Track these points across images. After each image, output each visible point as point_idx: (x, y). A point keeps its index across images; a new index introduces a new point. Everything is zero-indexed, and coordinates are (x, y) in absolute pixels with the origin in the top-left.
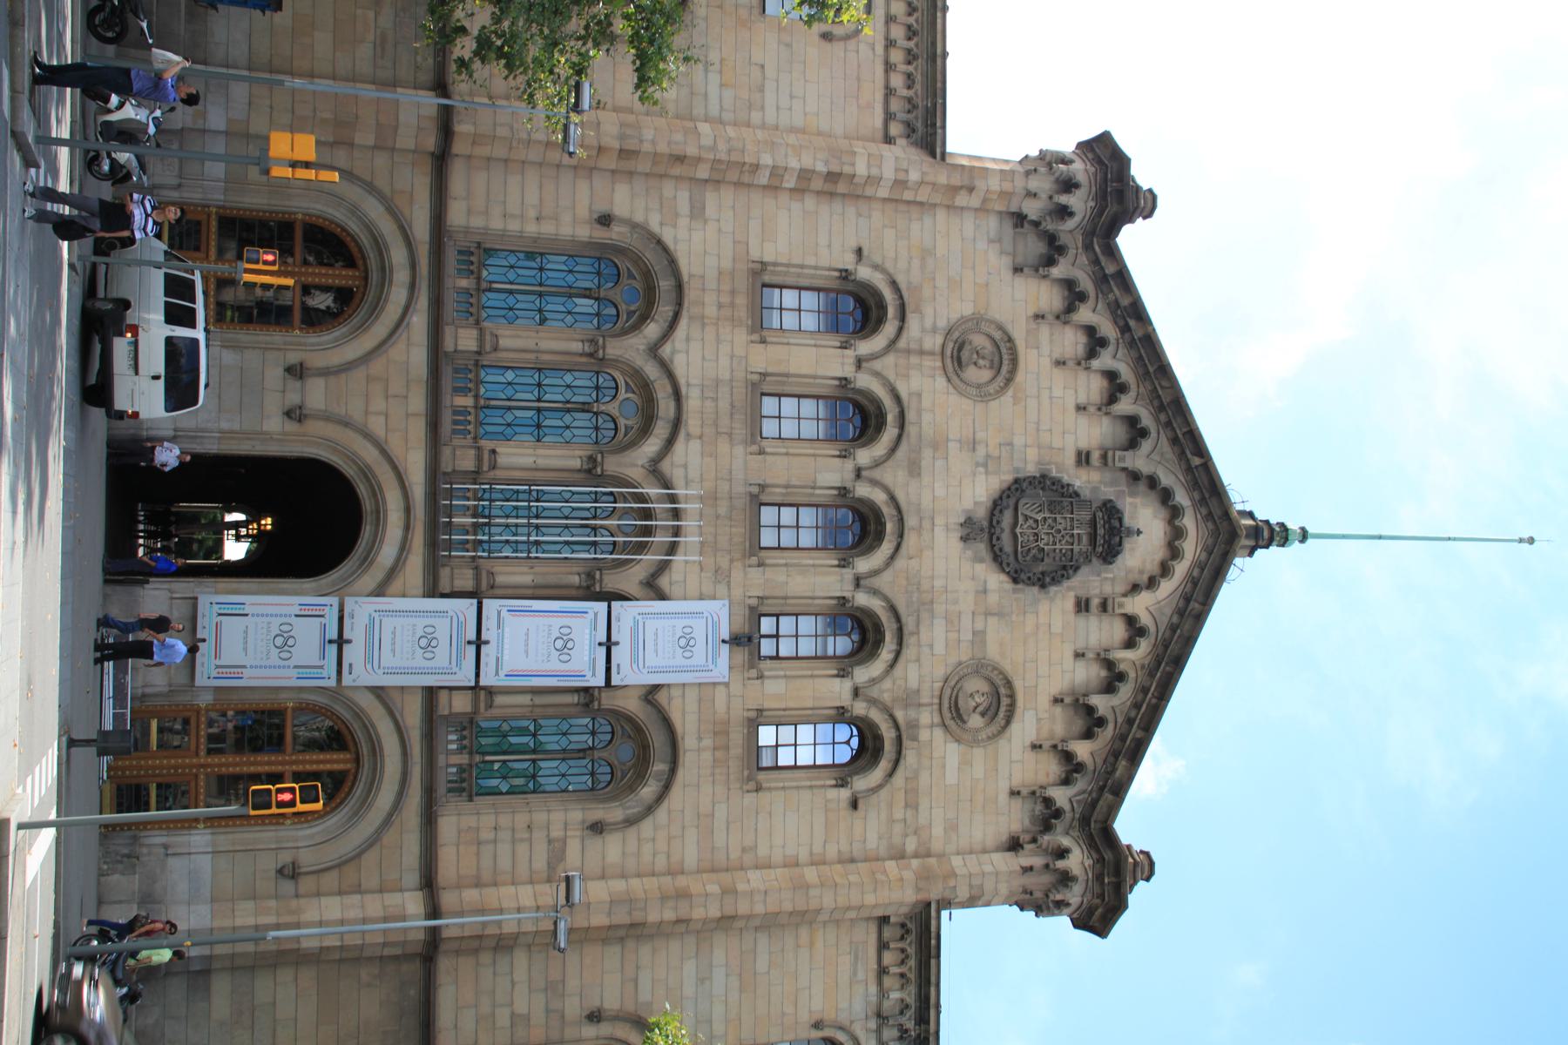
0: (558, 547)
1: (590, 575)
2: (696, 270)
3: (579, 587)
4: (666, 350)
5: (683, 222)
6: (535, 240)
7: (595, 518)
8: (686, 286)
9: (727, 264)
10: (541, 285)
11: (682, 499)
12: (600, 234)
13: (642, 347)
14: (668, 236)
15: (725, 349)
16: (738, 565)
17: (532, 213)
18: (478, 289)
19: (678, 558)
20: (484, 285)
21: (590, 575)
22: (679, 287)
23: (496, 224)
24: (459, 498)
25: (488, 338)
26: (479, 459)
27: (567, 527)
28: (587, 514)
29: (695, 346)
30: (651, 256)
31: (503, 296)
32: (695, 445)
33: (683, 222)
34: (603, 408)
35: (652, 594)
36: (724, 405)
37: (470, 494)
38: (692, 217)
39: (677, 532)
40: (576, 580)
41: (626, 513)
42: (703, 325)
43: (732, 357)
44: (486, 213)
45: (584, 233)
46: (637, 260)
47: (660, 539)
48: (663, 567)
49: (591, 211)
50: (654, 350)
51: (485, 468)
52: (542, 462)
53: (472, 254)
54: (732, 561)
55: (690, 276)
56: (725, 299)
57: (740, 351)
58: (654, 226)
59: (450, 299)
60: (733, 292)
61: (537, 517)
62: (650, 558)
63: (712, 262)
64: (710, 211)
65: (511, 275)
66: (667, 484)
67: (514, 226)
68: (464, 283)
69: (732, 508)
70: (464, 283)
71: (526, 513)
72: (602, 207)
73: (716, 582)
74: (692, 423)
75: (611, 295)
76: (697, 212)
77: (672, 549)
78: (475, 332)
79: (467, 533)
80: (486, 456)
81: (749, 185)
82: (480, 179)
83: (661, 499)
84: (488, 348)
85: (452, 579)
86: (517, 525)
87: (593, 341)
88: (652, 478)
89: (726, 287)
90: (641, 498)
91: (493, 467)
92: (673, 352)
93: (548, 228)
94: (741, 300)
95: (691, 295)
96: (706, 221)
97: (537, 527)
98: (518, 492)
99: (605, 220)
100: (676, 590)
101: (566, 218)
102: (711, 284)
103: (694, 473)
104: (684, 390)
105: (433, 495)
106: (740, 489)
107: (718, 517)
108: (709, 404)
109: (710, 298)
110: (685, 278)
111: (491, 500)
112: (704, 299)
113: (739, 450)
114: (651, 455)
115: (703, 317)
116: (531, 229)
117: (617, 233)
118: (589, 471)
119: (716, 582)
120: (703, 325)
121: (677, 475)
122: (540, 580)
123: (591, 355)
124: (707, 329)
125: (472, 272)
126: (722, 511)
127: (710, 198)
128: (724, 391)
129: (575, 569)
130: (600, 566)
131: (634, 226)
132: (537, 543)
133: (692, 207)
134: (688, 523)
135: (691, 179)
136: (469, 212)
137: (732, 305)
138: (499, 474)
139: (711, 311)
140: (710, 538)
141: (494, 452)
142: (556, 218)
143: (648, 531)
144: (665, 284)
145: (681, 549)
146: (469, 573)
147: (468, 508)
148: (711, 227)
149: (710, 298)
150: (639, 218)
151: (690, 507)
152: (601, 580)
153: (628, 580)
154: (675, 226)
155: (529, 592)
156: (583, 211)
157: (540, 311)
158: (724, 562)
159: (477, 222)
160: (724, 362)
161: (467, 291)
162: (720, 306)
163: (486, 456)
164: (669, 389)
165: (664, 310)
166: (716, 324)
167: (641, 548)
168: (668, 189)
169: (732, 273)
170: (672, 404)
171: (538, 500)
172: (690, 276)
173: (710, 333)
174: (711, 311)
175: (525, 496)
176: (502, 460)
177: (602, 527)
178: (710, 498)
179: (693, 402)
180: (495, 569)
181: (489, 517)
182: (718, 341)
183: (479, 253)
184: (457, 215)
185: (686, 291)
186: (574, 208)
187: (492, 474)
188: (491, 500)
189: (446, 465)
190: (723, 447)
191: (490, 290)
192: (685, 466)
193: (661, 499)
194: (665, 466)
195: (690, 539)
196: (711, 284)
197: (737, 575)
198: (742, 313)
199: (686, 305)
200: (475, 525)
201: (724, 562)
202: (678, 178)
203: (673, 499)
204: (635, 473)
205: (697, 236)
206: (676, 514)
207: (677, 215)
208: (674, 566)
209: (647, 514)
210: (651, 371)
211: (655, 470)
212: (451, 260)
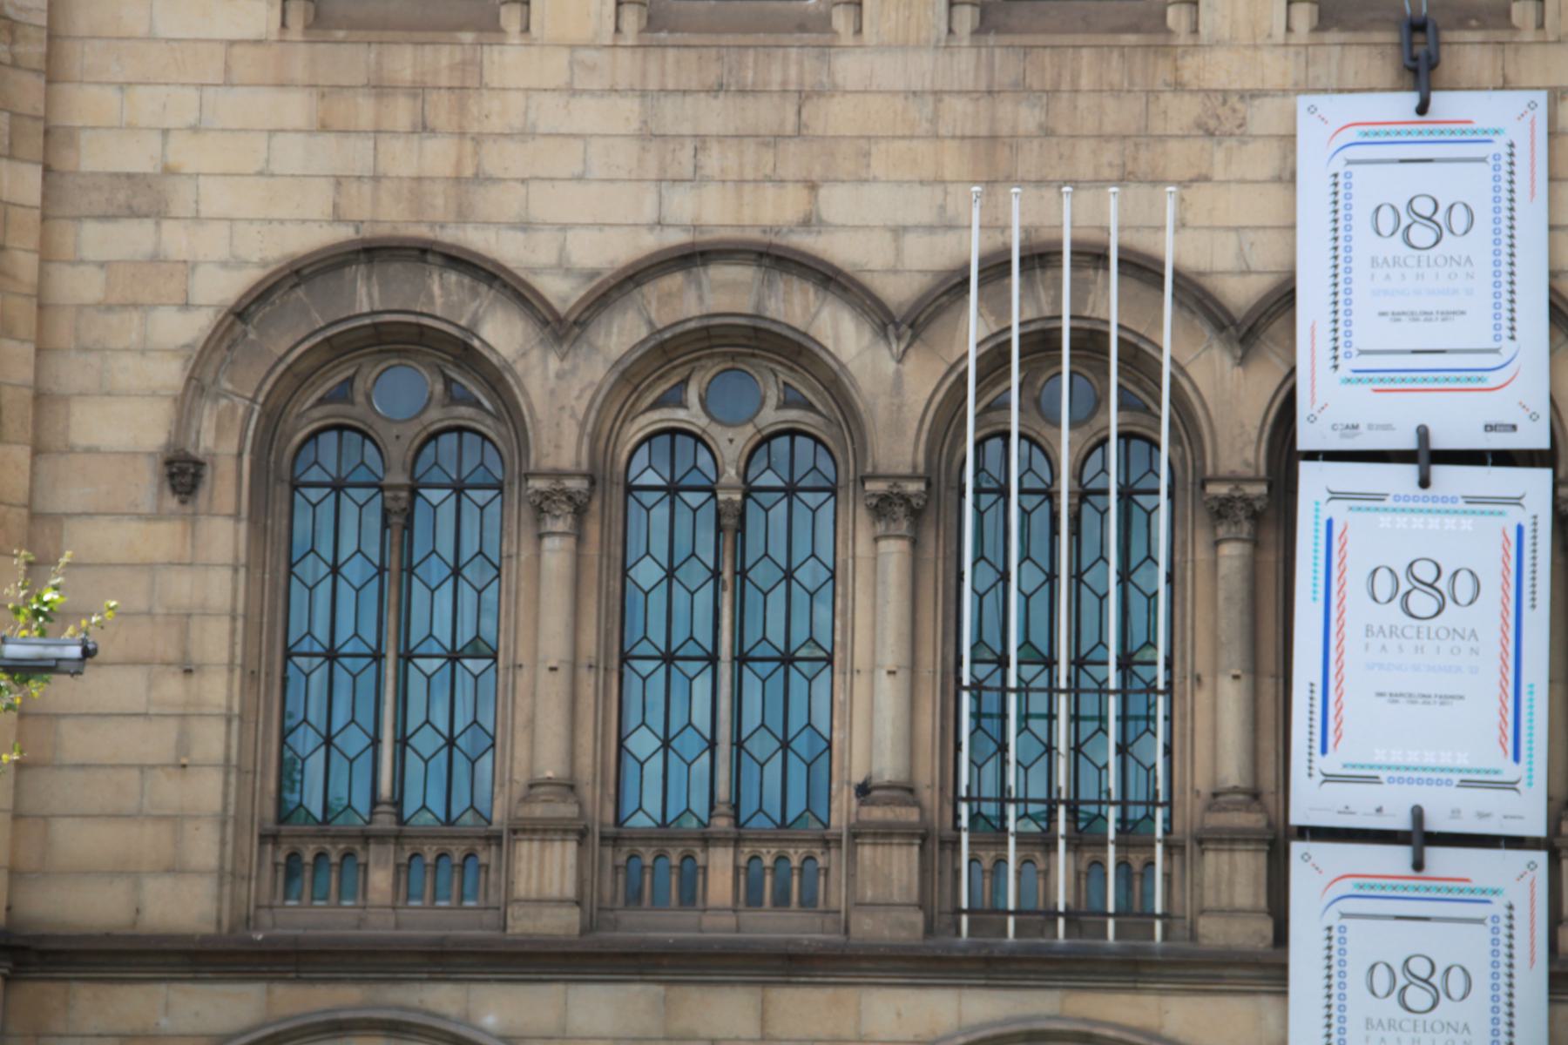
0: (1138, 603)
1: (1221, 511)
2: (318, 200)
3: (1256, 543)
4: (561, 291)
5: (176, 240)
6: (251, 676)
7: (1050, 495)
8: (367, 232)
9: (295, 107)
10: (377, 656)
11: (997, 240)
12: (226, 485)
13: (554, 364)
14: (223, 287)
15: (550, 114)
16: (1190, 67)
17: (173, 688)
18: (399, 838)
19: (1170, 251)
20: (385, 822)
21: (1221, 511)
22: (373, 252)
23: (208, 790)
24: (998, 889)
25: (538, 810)
26: (885, 833)
27: (1077, 577)
28: (1040, 518)
29: (548, 204)
30: (283, 339)
31: (414, 764)
32: (837, 203)
33: (176, 240)
34: (731, 474)
35: (1277, 326)
36: (714, 115)
37: (987, 858)
38: (158, 213)
39: (1091, 256)
40: (1232, 554)
41: (1039, 406)
42: (481, 179)
43: (572, 92)
44: (176, 820)
45: (224, 536)
46: (297, 378)
47: (1112, 302)
48: (1196, 297)
49: (157, 516)
50: (561, 329)
51: (912, 815)
52: (892, 652)
53: (294, 856)
54: (1178, 87)
55: (337, 218)
56: (401, 112)
57: (554, 68)
58: (194, 327)
59: (429, 919)
60: (380, 89)
61: (1050, 663)
62: (1169, 335)
63: (293, 154)
64: (138, 157)
65: (354, 741)
66: (952, 287)
67: (212, 740)
68: (380, 880)
69: (1020, 89)
70: (380, 880)
71: (1038, 703)
72: (145, 484)
73: (1241, 133)
74: (770, 212)
75: (398, 453)
76: (143, 198)
77: (1142, 269)
78: (526, 850)
79: (1100, 864)
80: (877, 814)
81: (53, 37)
82: (79, 840)
83: (996, 303)
84: (567, 810)
85: (1233, 912)
86: (1075, 718)
87: (540, 508)
88: (936, 331)
89: (365, 110)
90: (994, 362)
91: (906, 791)
92: (563, 268)
93: (216, 641)
94: (404, 62)
95: (392, 217)
96: (168, 171)
97: (1078, 662)
98: (977, 715)
99: (183, 474)
100: (1265, 256)
101: (182, 588)
102: (356, 155)
103: (919, 207)
104: (675, 238)
105: (991, 968)
106: (964, 65)
107: (1047, 132)
108: (713, 161)
109: (402, 159)
110: (344, 233)
111: (1003, 799)
112: (398, 175)
113: (849, 68)
114: (867, 335)
115: (458, 180)
116: (217, 689)
117: (221, 439)
118: (916, 515)
119: (1241, 133)
120: (481, 179)
121: (926, 257)
122: (1234, 657)
123: (580, 512)
124: (492, 165)
125: (348, 855)
126: (1028, 118)
127: (99, 155)
128: (677, 116)
129: (1202, 554)
130: (1191, 480)
131: (196, 387)
132: (1125, 663)
133: (133, 213)
134: (1067, 218)
135: (44, 218)
136: (175, 869)
137: (418, 90)
138: (927, 774)
139: (438, 156)
140: (1111, 153)
141: (864, 790)
142: (184, 618)
143: (1090, 341)
144: (366, 296)
145: (1143, 242)
146: (1214, 863)
147: (1024, 861)
148: (185, 154)
149: (402, 159)
150: (171, 374)
151: (1019, 215)
152: (1235, 480)
153: (1232, 395)
154: (190, 266)
155: (1269, 687)
156: (162, 539)
157: (454, 657)
158: (1182, 111)
159: (204, 847)
160: (588, 115)
161: (402, 871)
162: (424, 128)
163: (877, 814)
164: (675, 280)
165: (442, 298)
166: (478, 139)
167: (1139, 362)
168: (78, 285)
169: (326, 91)
170: (720, 273)
171: (1003, 662)
172: (337, 218)
173: (496, 159)
174: (438, 156)
175: (990, 702)
176: (888, 767)
177: (1077, 474)
178: (993, 159)
179: (712, 211)
180: (1203, 783)
181: (1051, 804)
182: (526, 134)
183: (292, 837)
184: (186, 905)
185: (383, 231)
186: (150, 566)
187: (929, 796)
188: (1003, 799)
189: (904, 928)
190: (837, 116)
191: (398, 802)
192: (898, 231)
193: (996, 303)
194: (898, 291)
195: (1113, 216)
196: (356, 155)
197: (1219, 69)
198: (442, 59)
199: (423, 232)
200: (1074, 845)
201: (1182, 111)
202: (46, 256)
203: (994, 268)
204: (920, 380)
205: (217, 197)
206: (1040, 258)
207: (156, 259)
208: (1192, 262)
209: (1041, 343)
210: (622, 334)
211: (912, 322)
212: (310, 917)
